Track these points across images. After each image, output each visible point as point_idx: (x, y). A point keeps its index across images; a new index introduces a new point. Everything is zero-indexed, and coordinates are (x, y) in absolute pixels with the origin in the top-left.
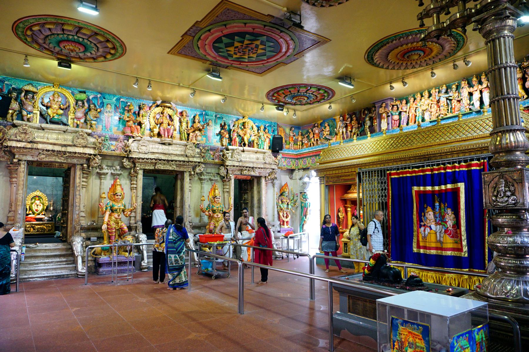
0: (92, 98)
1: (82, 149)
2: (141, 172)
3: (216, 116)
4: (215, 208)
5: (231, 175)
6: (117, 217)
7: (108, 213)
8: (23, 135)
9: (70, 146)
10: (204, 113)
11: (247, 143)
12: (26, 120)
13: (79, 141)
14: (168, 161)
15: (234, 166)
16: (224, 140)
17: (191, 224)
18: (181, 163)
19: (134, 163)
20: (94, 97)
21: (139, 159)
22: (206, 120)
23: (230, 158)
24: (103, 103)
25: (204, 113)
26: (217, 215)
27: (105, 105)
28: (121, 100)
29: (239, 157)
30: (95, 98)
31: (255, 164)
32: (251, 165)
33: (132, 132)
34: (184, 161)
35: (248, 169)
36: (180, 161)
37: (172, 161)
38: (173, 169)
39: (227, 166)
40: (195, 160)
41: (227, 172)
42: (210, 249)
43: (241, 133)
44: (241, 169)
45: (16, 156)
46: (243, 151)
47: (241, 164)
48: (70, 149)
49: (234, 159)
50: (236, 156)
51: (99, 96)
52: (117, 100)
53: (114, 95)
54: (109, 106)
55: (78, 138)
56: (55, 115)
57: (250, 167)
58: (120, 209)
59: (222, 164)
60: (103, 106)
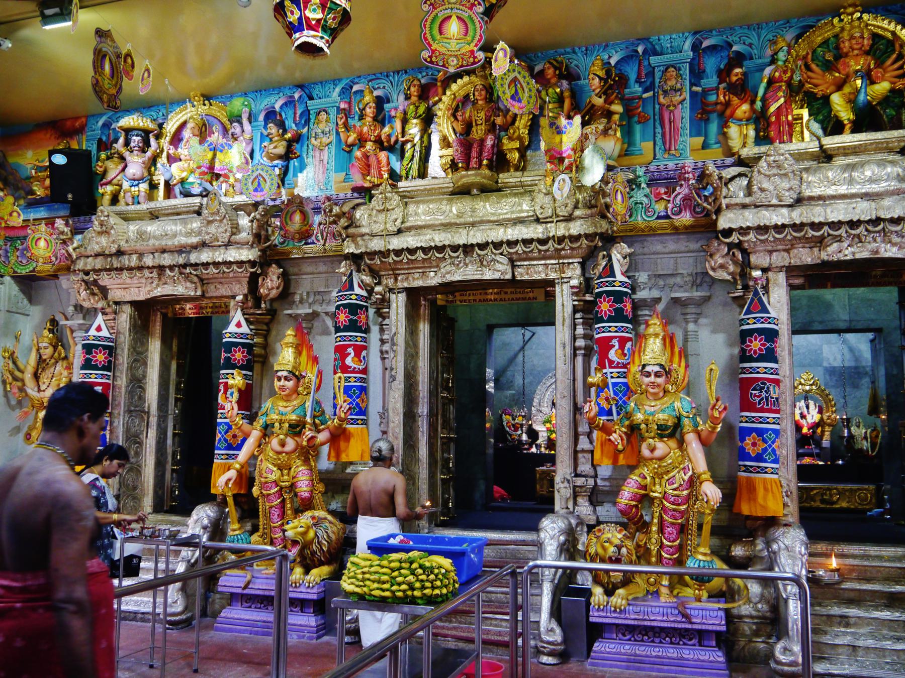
0: (281, 107)
1: (222, 250)
2: (399, 303)
3: (695, 47)
4: (639, 417)
5: (757, 274)
6: (279, 448)
7: (255, 434)
8: (103, 240)
9: (195, 247)
10: (640, 49)
11: (845, 114)
12: (130, 201)
13: (212, 229)
14: (467, 249)
15: (762, 229)
16: (733, 130)
17: (580, 481)
18: (520, 248)
19: (374, 273)
20: (285, 104)
21: (372, 254)
22: (651, 74)
23: (741, 197)
24: (307, 112)
25: (640, 49)
26: (653, 450)
27: (312, 117)
28: (355, 88)
29: (785, 185)
30: (290, 103)
31: (887, 202)
32: (863, 210)
33: (364, 176)
34: (527, 242)
35: (842, 232)
36: (511, 243)
37: (483, 246)
38: (497, 276)
39: (728, 232)
40: (576, 228)
41: (746, 266)
42: (609, 592)
43: (821, 82)
44: (818, 234)
45: (111, 295)
46: (826, 156)
47: (798, 216)
48: (194, 258)
49: (758, 197)
50: (772, 184)
51: (296, 96)
52: (344, 91)
53: (335, 81)
54: (323, 116)
55: (210, 222)
56: (184, 174)
57: (859, 222)
58: (281, 422)
59: (706, 228)
60: (308, 121)
